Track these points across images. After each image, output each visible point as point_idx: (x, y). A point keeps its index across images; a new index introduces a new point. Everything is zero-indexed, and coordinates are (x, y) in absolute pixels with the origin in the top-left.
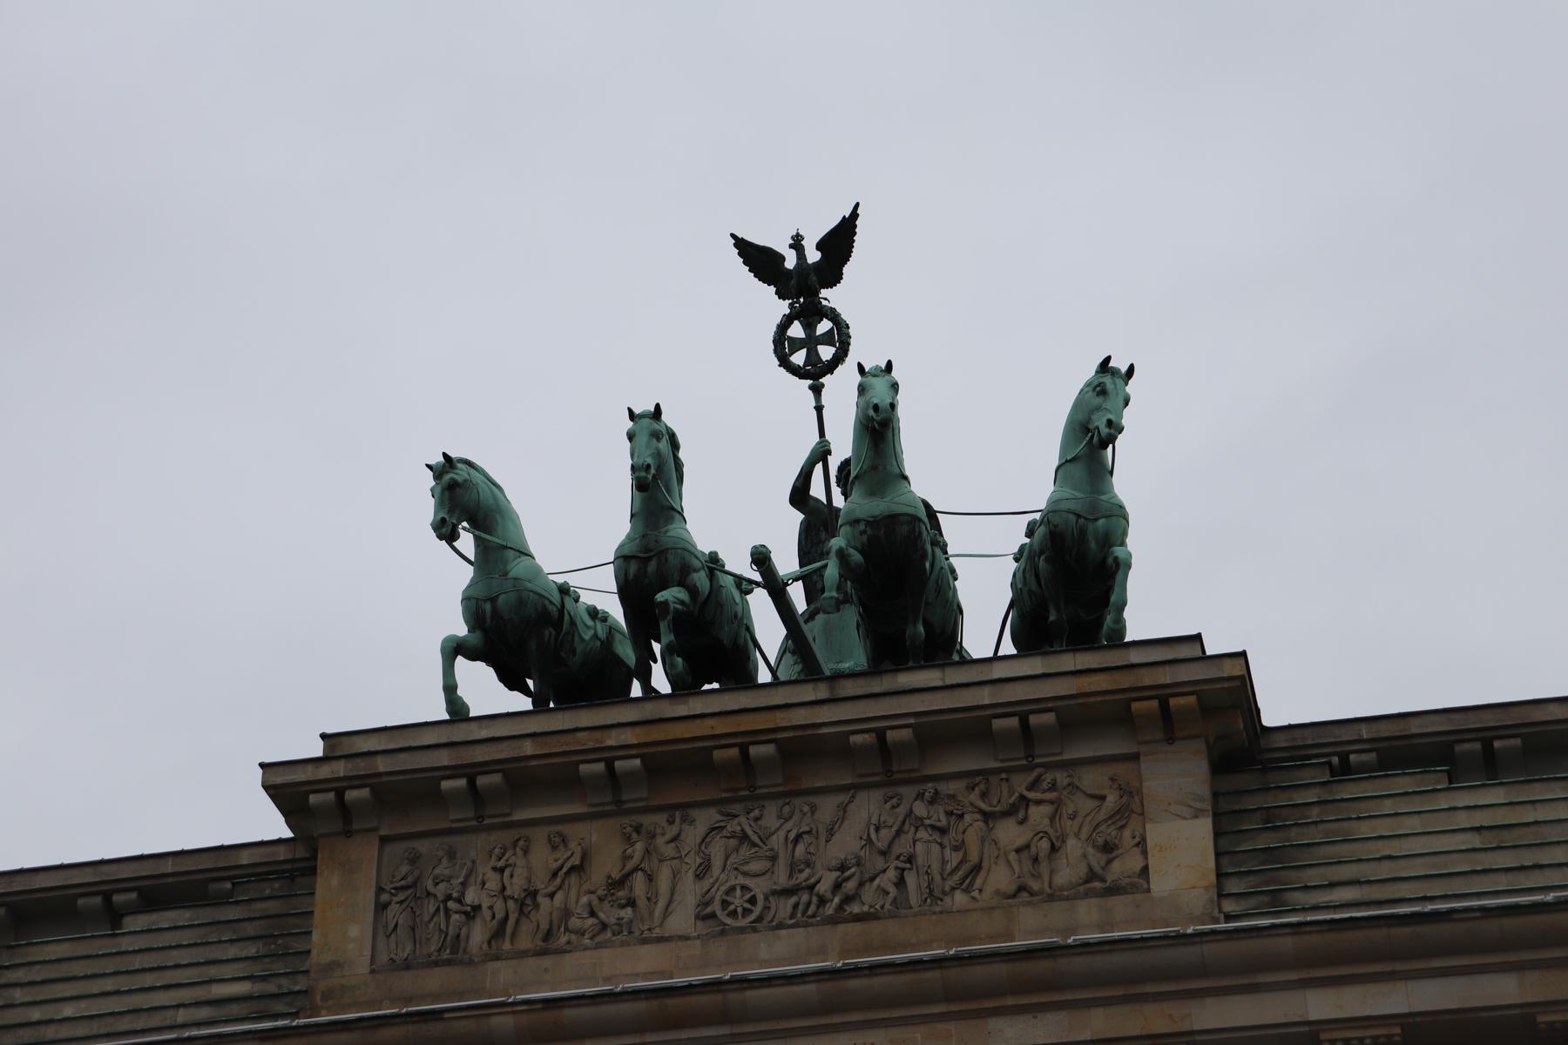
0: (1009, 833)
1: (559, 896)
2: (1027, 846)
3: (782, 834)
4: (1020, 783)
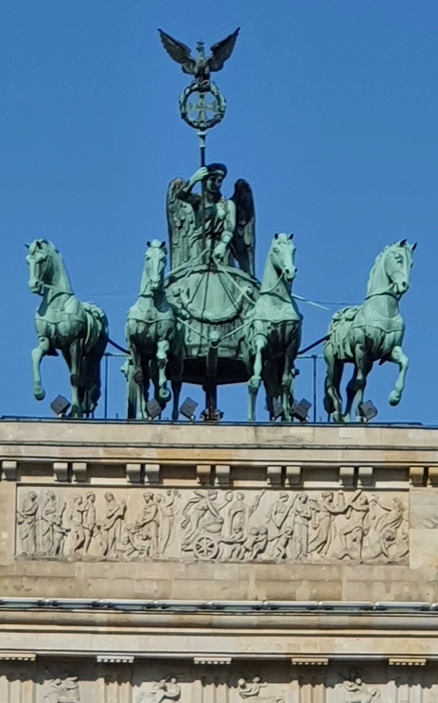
1: (112, 530)
2: (350, 532)
3: (227, 508)
4: (349, 495)
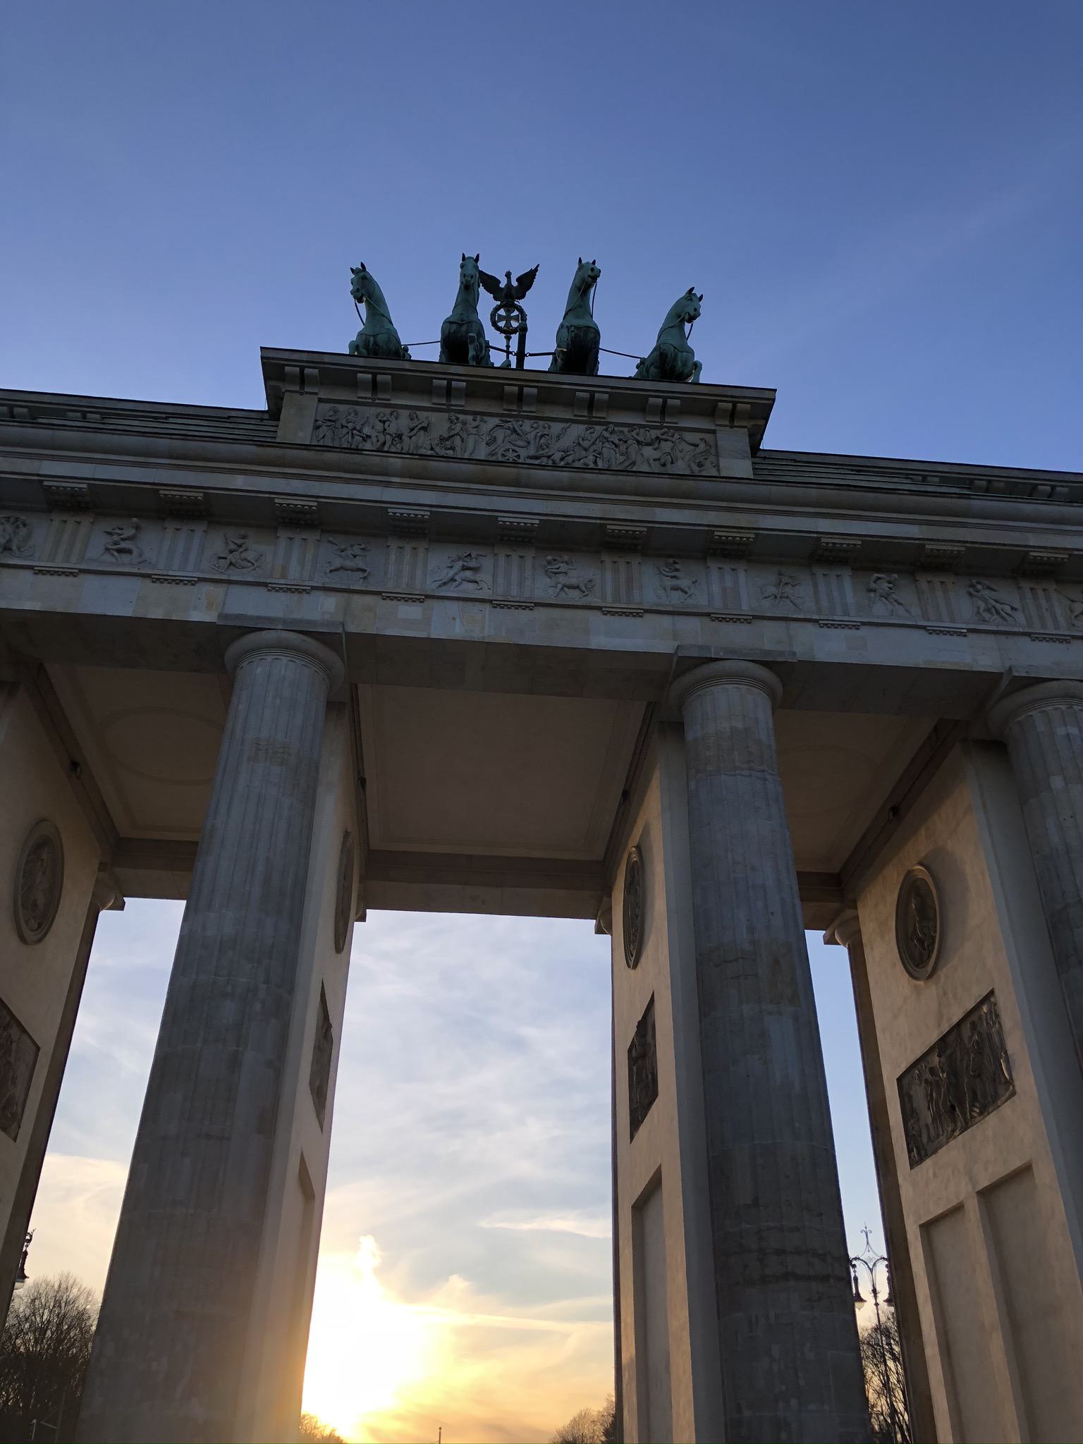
0: (648, 452)
4: (654, 433)
